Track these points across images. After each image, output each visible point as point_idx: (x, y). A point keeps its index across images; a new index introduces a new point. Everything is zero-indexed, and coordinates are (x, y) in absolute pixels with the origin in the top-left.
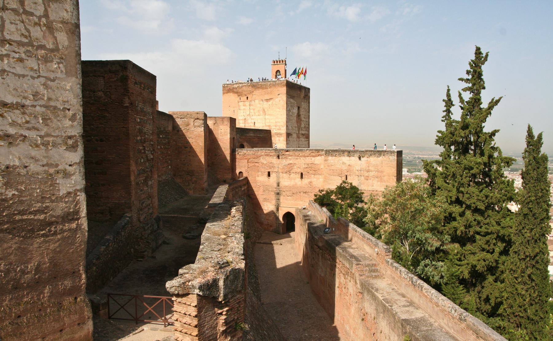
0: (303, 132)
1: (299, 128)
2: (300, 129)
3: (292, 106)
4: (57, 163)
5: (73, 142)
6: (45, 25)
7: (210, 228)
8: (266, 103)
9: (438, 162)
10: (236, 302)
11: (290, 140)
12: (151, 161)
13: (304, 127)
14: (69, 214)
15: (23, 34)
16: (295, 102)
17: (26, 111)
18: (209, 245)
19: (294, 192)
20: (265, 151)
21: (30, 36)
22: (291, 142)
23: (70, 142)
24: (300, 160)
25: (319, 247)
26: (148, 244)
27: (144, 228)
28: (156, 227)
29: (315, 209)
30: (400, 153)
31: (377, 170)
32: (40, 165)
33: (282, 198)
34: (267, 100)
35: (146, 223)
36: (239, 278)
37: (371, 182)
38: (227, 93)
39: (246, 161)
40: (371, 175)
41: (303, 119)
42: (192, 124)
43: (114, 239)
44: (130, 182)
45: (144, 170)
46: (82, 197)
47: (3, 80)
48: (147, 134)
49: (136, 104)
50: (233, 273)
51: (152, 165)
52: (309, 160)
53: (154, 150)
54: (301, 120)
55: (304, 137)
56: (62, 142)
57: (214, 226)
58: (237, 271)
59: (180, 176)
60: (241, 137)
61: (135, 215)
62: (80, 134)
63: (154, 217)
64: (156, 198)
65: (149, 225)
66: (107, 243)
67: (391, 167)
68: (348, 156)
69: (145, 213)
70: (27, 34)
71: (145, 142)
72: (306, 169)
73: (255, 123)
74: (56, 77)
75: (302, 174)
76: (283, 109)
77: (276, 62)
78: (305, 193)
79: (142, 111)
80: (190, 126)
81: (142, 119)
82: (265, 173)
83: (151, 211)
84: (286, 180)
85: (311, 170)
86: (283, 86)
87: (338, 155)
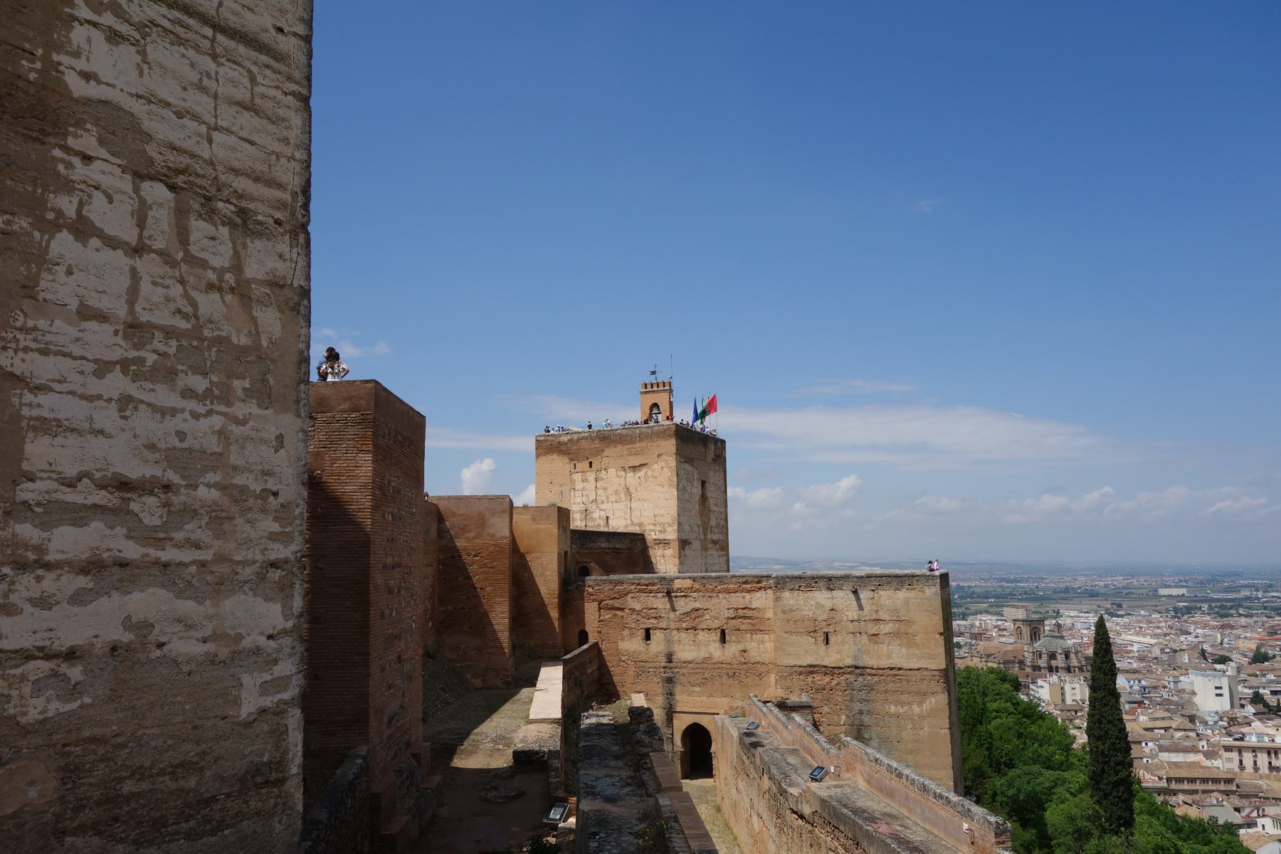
0: (715, 537)
1: (705, 528)
2: (707, 529)
3: (688, 480)
4: (237, 631)
5: (280, 577)
6: (232, 290)
14: (257, 769)
15: (179, 311)
17: (174, 498)
21: (196, 316)
23: (276, 575)
24: (718, 601)
25: (802, 817)
30: (944, 578)
32: (197, 639)
33: (678, 689)
34: (634, 468)
38: (546, 454)
41: (713, 508)
46: (295, 718)
47: (124, 421)
52: (738, 600)
54: (710, 511)
55: (718, 546)
56: (253, 577)
62: (298, 554)
67: (928, 611)
70: (189, 309)
72: (734, 621)
73: (607, 518)
74: (250, 414)
76: (670, 485)
77: (649, 386)
82: (639, 633)
84: (687, 647)
86: (670, 436)
87: (805, 587)
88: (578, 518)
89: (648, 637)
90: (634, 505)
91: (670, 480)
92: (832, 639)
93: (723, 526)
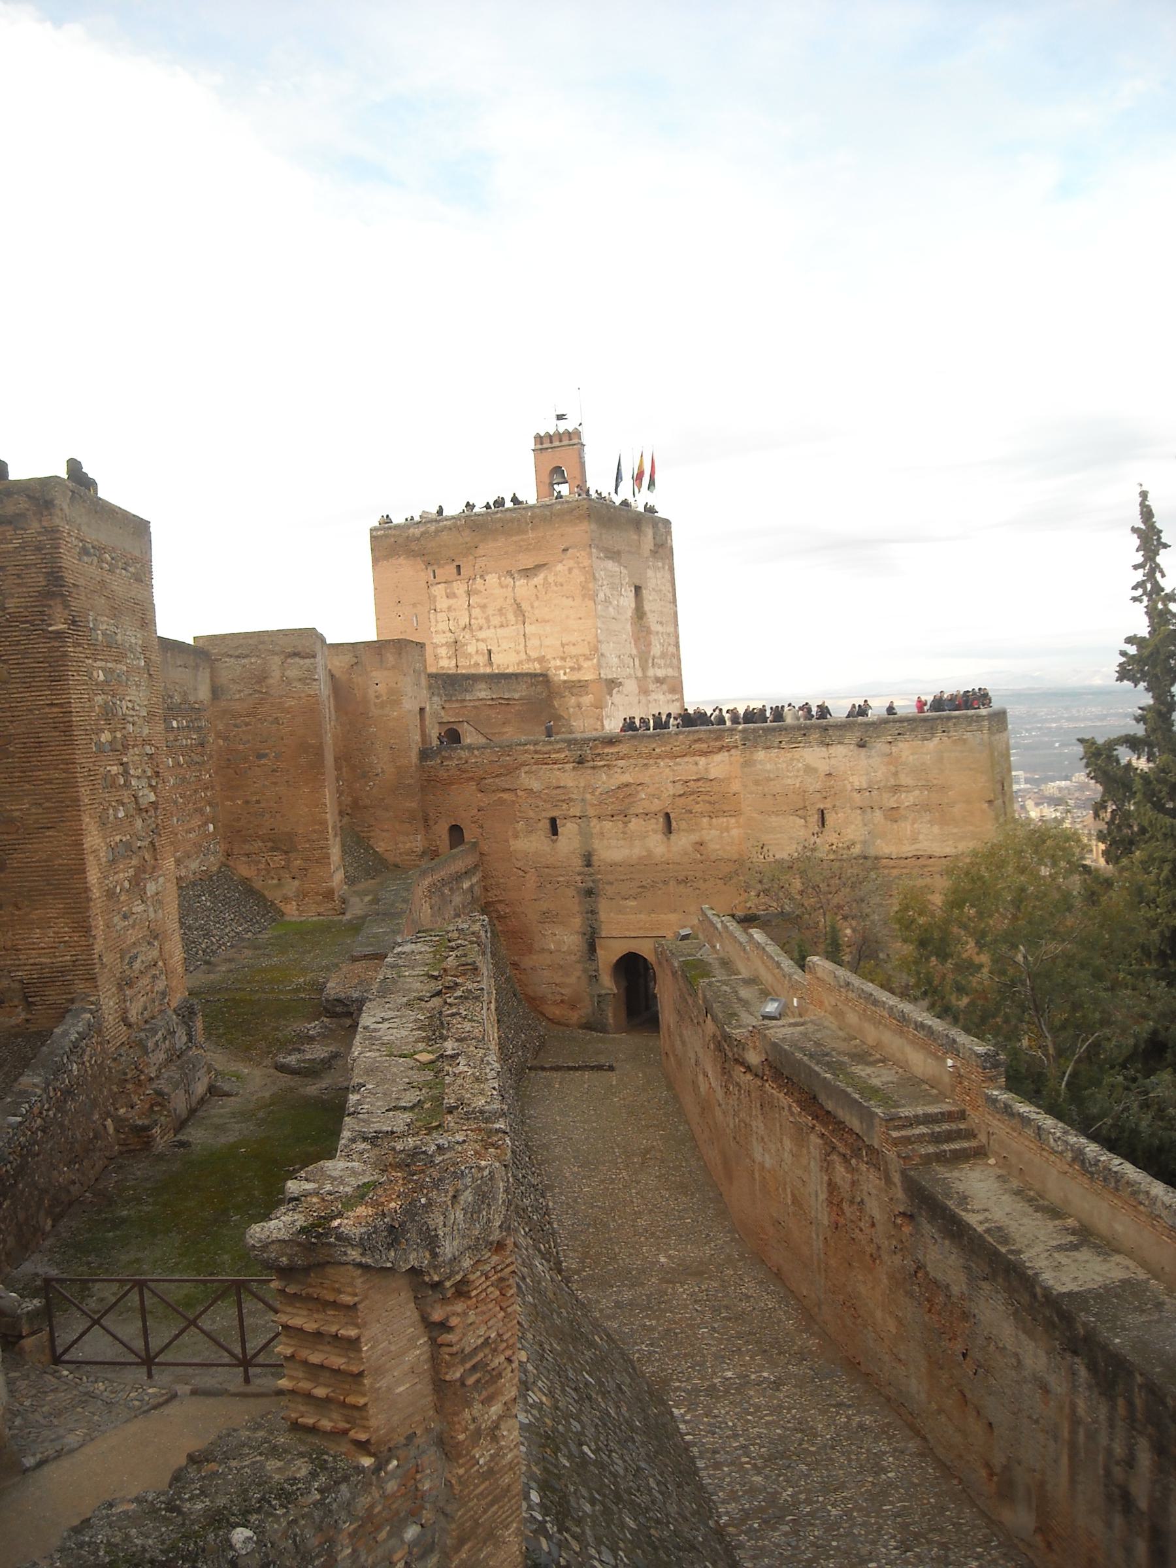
0: (660, 673)
1: (644, 658)
2: (647, 661)
7: (375, 1030)
8: (523, 581)
9: (1133, 743)
10: (488, 1283)
11: (616, 702)
12: (152, 813)
13: (662, 653)
16: (624, 571)
18: (380, 1089)
19: (644, 883)
20: (532, 748)
22: (621, 708)
25: (749, 1069)
26: (160, 1099)
27: (141, 1044)
28: (181, 1039)
29: (724, 935)
31: (924, 783)
34: (527, 573)
35: (148, 1026)
36: (494, 1198)
37: (909, 827)
38: (387, 557)
39: (472, 786)
40: (907, 804)
41: (655, 627)
42: (277, 674)
43: (45, 1090)
44: (87, 890)
45: (128, 846)
48: (131, 719)
49: (88, 621)
50: (473, 1182)
51: (154, 826)
52: (689, 767)
53: (157, 774)
54: (649, 632)
55: (665, 687)
57: (386, 1025)
58: (486, 1173)
59: (248, 855)
60: (447, 706)
61: (111, 1003)
63: (174, 1005)
64: (177, 937)
65: (160, 1033)
66: (27, 1106)
67: (971, 769)
68: (822, 742)
69: (143, 992)
71: (126, 747)
72: (682, 800)
73: (490, 652)
75: (667, 815)
76: (584, 596)
78: (685, 881)
79: (110, 644)
80: (271, 681)
81: (112, 671)
82: (540, 825)
83: (161, 985)
84: (613, 842)
85: (698, 803)
87: (787, 742)
88: (444, 655)
89: (554, 831)
90: (530, 629)
91: (583, 587)
92: (830, 818)
93: (673, 655)
